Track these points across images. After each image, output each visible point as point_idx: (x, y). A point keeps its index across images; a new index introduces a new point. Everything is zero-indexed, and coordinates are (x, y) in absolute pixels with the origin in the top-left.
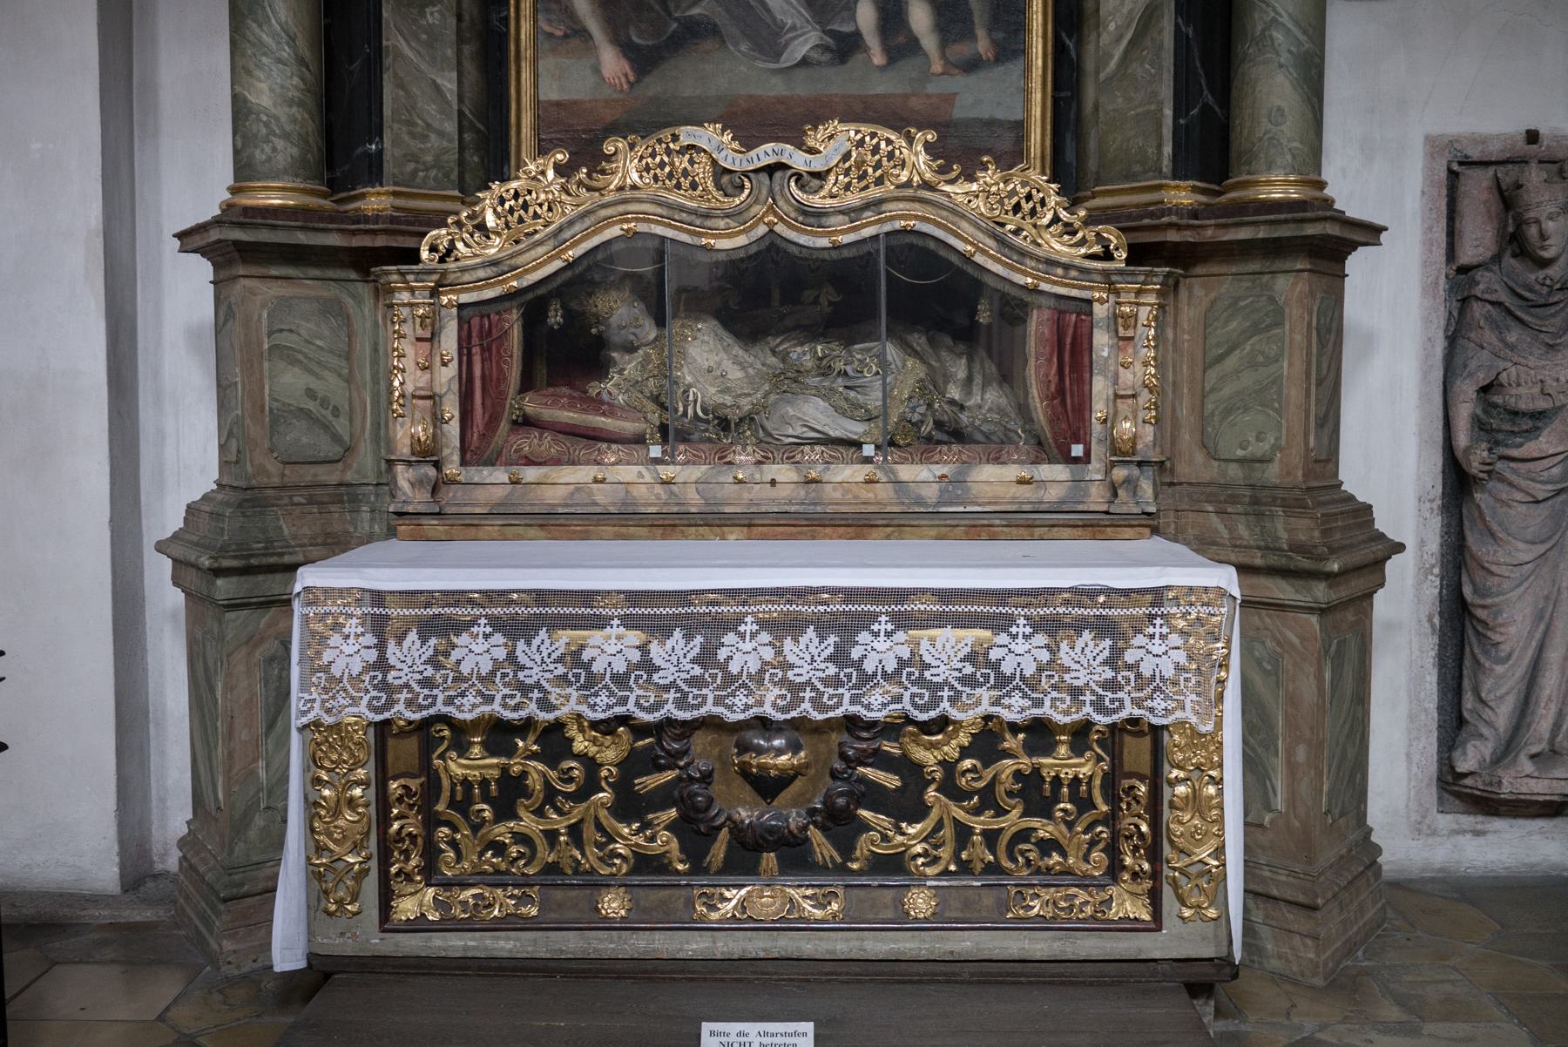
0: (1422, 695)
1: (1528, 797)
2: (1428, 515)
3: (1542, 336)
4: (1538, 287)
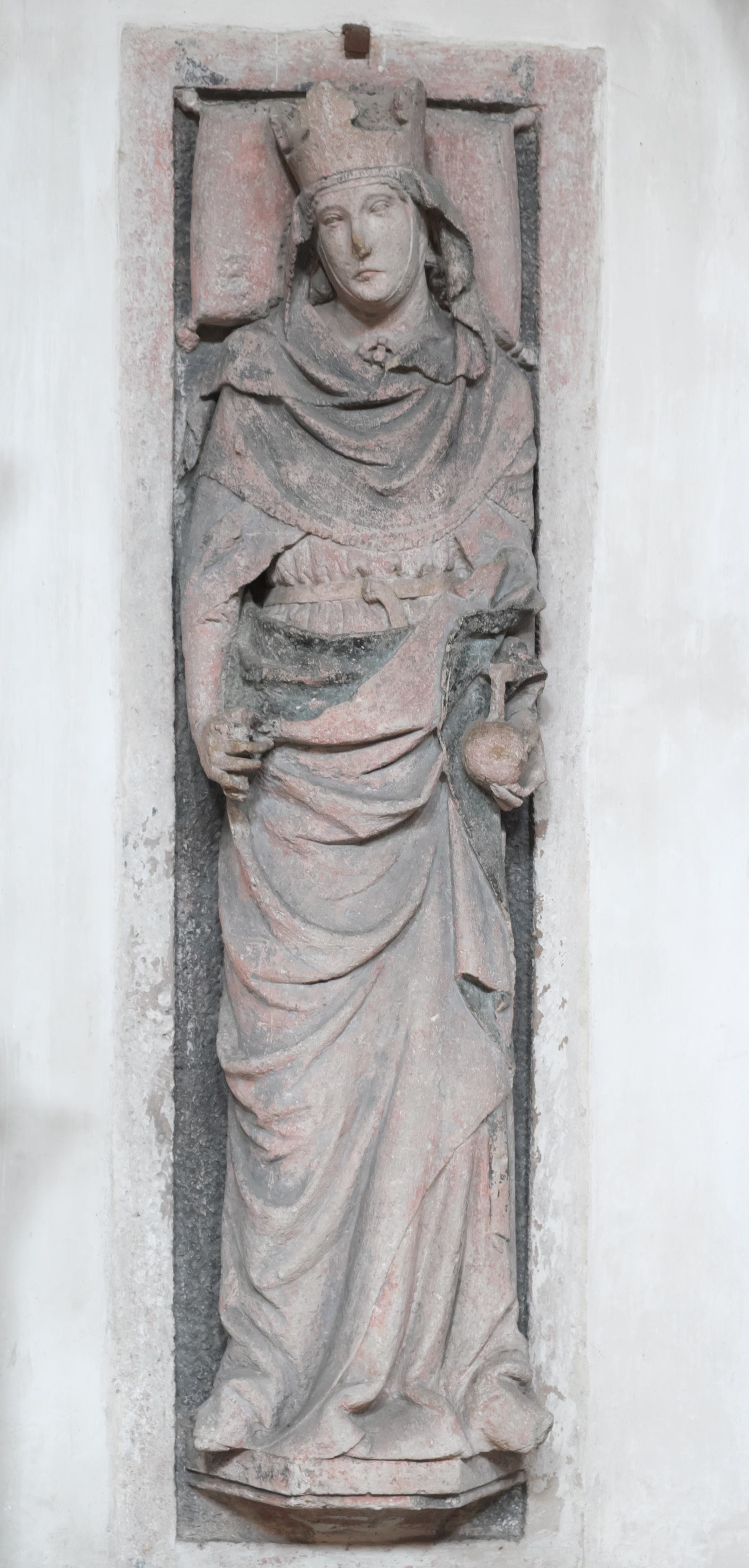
0: (140, 1278)
1: (349, 1503)
2: (145, 876)
3: (362, 471)
4: (356, 366)
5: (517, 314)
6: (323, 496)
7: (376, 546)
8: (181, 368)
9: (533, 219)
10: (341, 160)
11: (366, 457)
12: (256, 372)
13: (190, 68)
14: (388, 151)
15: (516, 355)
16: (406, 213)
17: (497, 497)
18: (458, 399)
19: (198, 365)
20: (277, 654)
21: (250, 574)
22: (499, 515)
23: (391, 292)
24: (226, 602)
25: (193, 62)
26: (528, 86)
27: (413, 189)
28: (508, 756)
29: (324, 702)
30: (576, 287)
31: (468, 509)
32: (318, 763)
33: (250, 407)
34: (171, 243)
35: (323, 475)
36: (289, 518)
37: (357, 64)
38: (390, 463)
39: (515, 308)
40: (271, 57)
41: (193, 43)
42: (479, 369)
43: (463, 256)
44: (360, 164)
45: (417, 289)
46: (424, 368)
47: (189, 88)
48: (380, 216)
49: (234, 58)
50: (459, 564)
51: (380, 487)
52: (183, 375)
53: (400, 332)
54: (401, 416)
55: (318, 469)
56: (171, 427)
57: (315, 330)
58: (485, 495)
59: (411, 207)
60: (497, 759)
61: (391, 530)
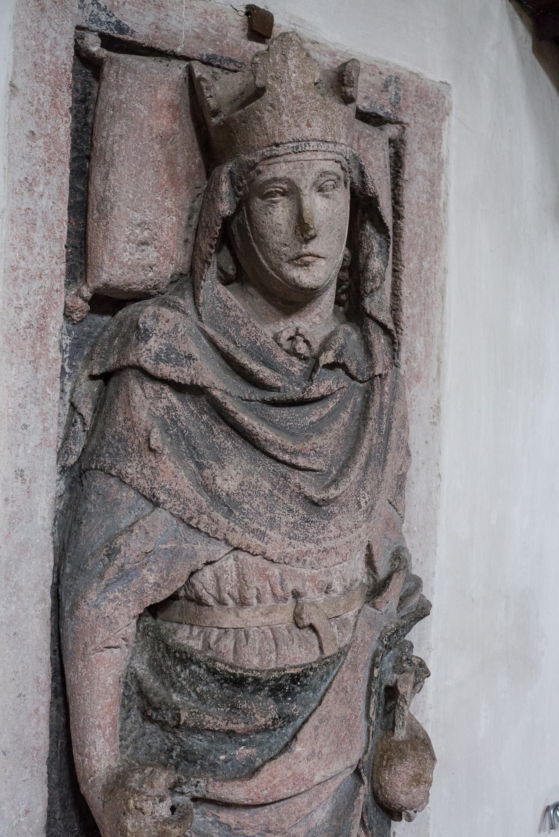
3: (296, 478)
4: (282, 357)
6: (255, 505)
10: (299, 126)
11: (301, 461)
12: (173, 356)
20: (195, 690)
21: (160, 592)
26: (395, 104)
28: (425, 782)
29: (254, 750)
30: (427, 294)
32: (242, 821)
33: (163, 395)
34: (66, 198)
35: (253, 481)
37: (258, 47)
38: (324, 469)
40: (178, 19)
43: (381, 251)
44: (318, 135)
47: (93, 31)
48: (327, 197)
49: (141, 11)
51: (317, 497)
53: (314, 323)
55: (248, 474)
57: (232, 313)
60: (415, 787)
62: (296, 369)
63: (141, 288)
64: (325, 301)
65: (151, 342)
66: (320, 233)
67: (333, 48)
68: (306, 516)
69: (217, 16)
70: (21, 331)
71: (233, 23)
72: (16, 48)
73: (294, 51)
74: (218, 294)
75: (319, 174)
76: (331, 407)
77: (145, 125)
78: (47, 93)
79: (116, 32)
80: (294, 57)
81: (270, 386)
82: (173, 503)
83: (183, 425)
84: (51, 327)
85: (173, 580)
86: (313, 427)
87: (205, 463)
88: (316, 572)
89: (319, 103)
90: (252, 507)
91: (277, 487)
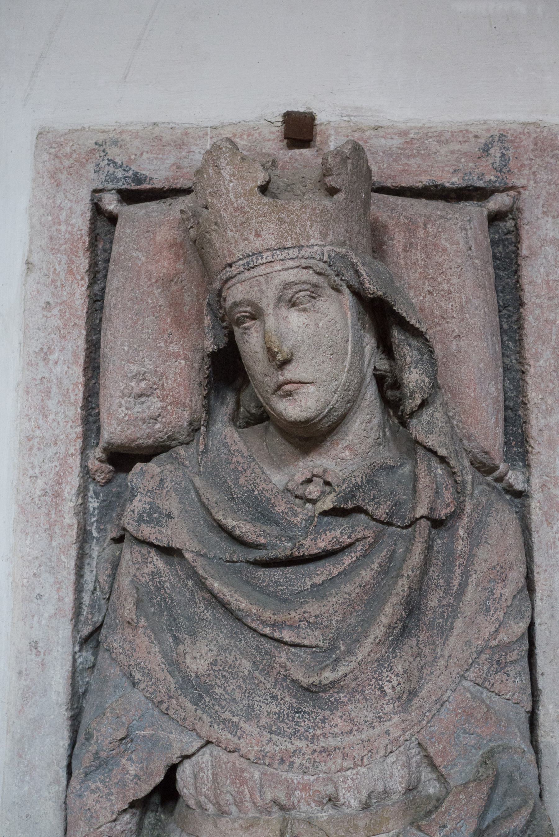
4: (281, 507)
5: (500, 430)
6: (229, 689)
7: (301, 766)
8: (93, 504)
9: (514, 318)
10: (246, 239)
11: (287, 635)
12: (155, 515)
13: (111, 169)
14: (311, 227)
15: (499, 480)
16: (341, 306)
17: (479, 677)
18: (418, 548)
19: (114, 499)
22: (483, 701)
23: (323, 409)
24: (115, 821)
25: (115, 163)
27: (349, 274)
31: (436, 702)
33: (150, 560)
34: (81, 360)
35: (230, 660)
36: (185, 719)
37: (301, 154)
38: (321, 644)
39: (497, 422)
41: (115, 143)
42: (448, 505)
43: (421, 359)
44: (272, 243)
45: (364, 404)
46: (370, 509)
48: (304, 310)
49: (161, 156)
50: (426, 774)
51: (305, 681)
52: (96, 512)
54: (340, 574)
55: (225, 651)
56: (72, 577)
57: (235, 459)
58: (462, 676)
59: (348, 298)
61: (323, 743)
62: (299, 520)
63: (150, 441)
64: (353, 431)
65: (136, 502)
66: (297, 355)
67: (403, 127)
68: (295, 705)
69: (248, 136)
70: (37, 500)
71: (267, 136)
72: (32, 227)
73: (225, 159)
74: (225, 438)
75: (282, 287)
76: (347, 563)
77: (143, 272)
78: (63, 262)
79: (133, 184)
80: (227, 165)
81: (253, 543)
82: (145, 683)
83: (166, 593)
84: (66, 493)
85: (151, 774)
86: (318, 591)
87: (181, 636)
88: (312, 778)
89: (267, 207)
90: (226, 692)
91: (260, 668)
